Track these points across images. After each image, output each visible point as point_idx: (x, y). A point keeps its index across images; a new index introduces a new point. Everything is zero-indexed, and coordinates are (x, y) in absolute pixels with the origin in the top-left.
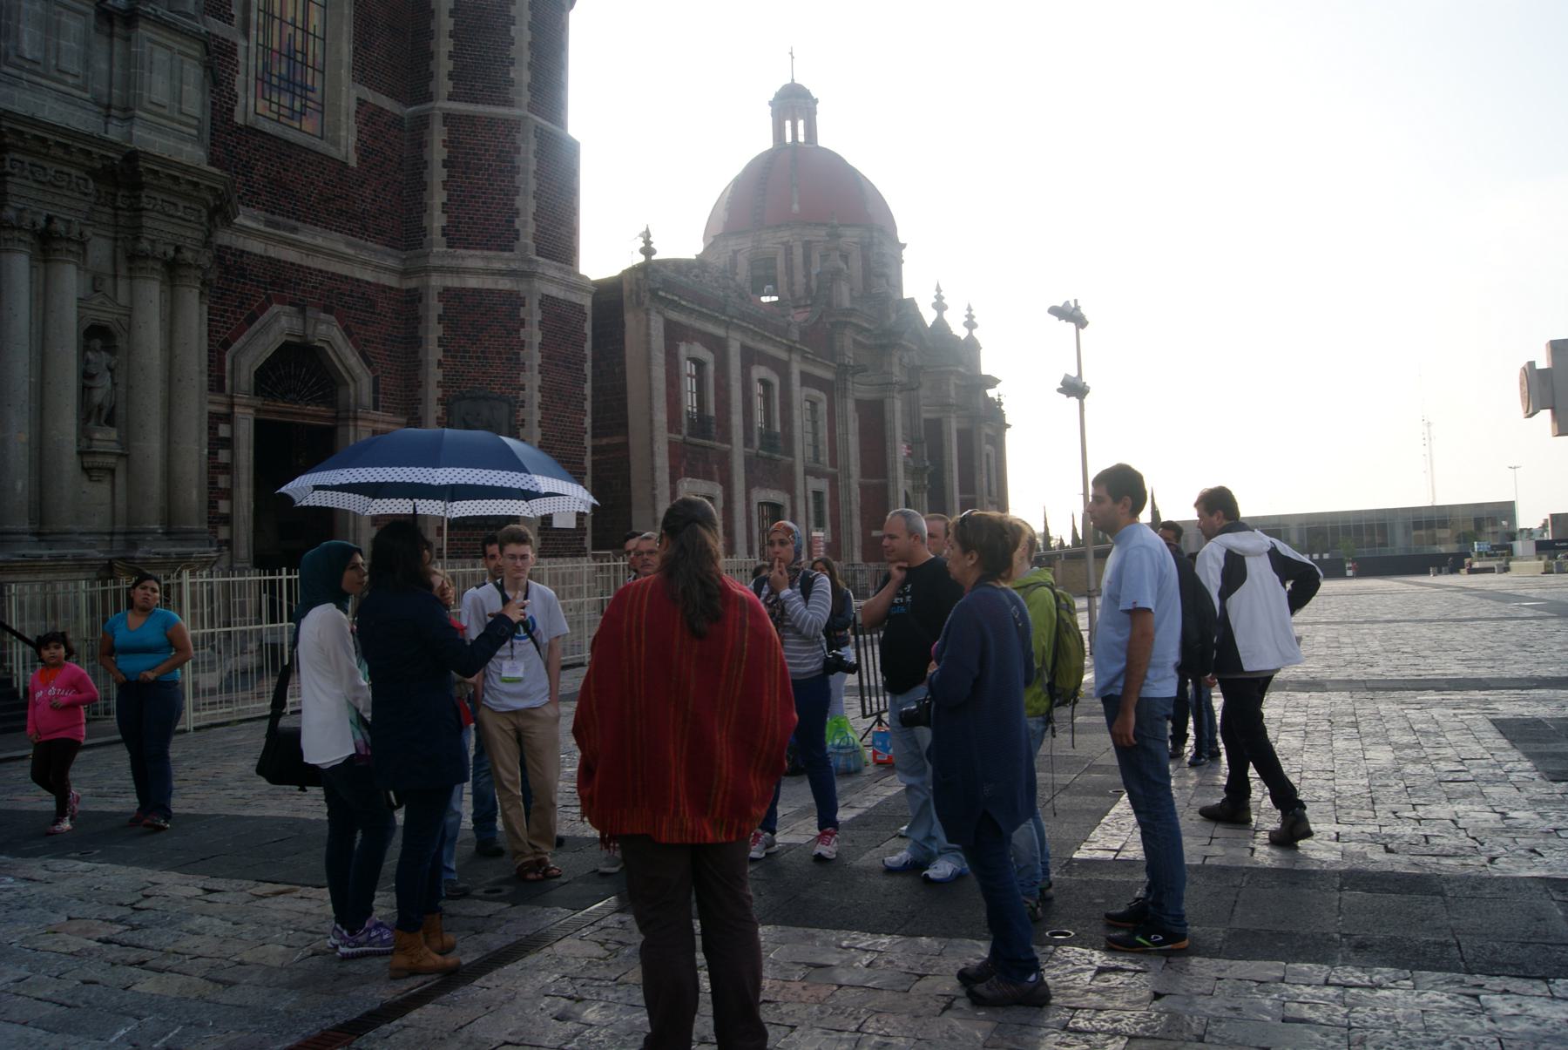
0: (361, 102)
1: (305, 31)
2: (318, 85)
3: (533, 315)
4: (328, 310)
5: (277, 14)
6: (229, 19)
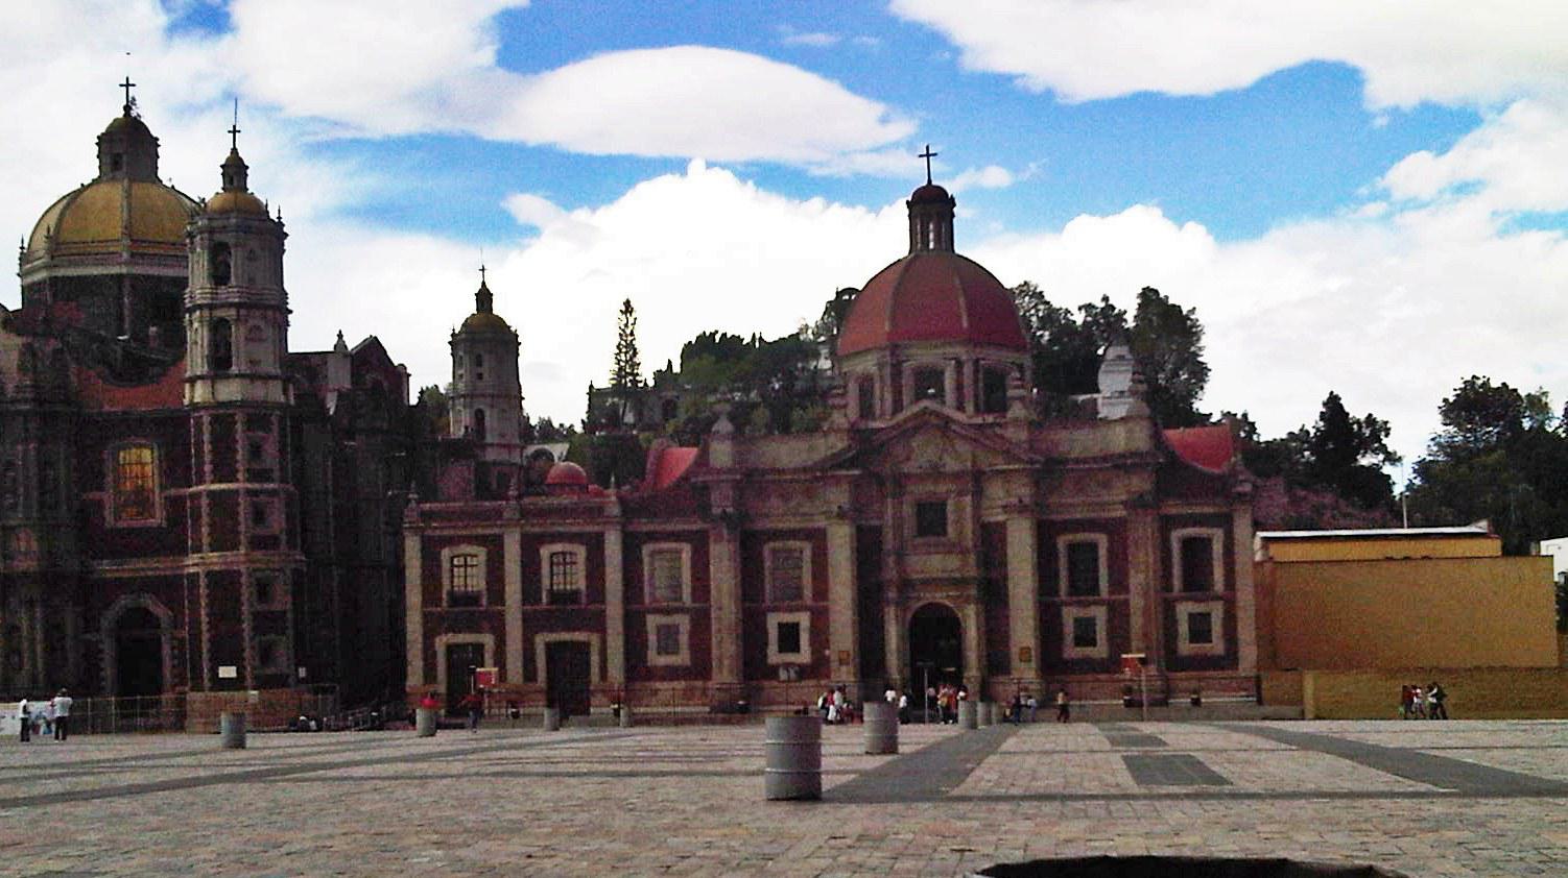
1: (144, 477)
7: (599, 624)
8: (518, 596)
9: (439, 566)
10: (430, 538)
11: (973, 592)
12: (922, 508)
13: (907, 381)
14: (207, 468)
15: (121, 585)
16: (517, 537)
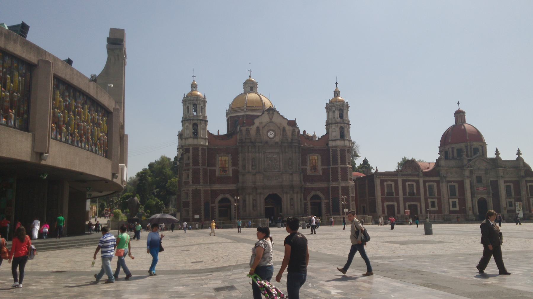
0: (322, 168)
1: (315, 163)
2: (317, 168)
3: (340, 188)
4: (319, 191)
5: (312, 162)
6: (306, 166)
7: (419, 200)
8: (402, 194)
9: (384, 187)
10: (382, 180)
11: (491, 195)
12: (477, 177)
13: (472, 150)
14: (339, 161)
15: (313, 189)
16: (401, 180)
